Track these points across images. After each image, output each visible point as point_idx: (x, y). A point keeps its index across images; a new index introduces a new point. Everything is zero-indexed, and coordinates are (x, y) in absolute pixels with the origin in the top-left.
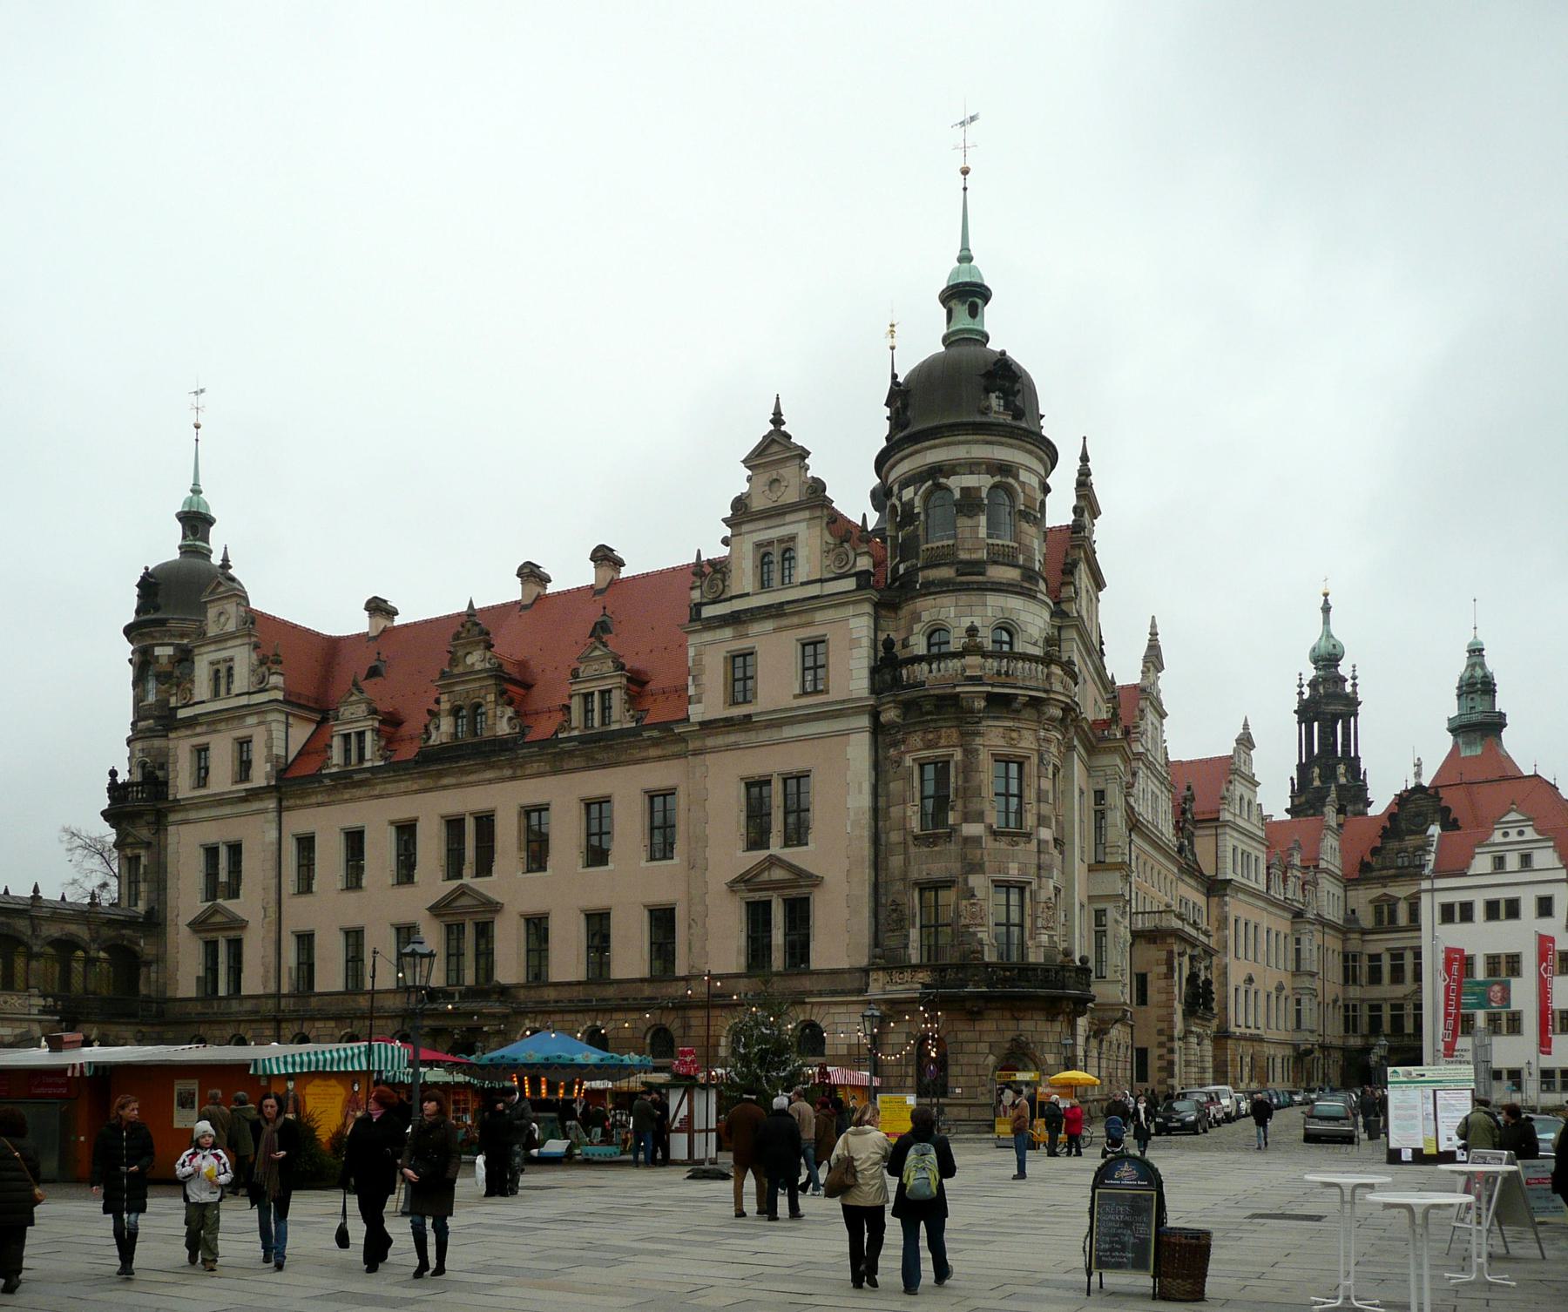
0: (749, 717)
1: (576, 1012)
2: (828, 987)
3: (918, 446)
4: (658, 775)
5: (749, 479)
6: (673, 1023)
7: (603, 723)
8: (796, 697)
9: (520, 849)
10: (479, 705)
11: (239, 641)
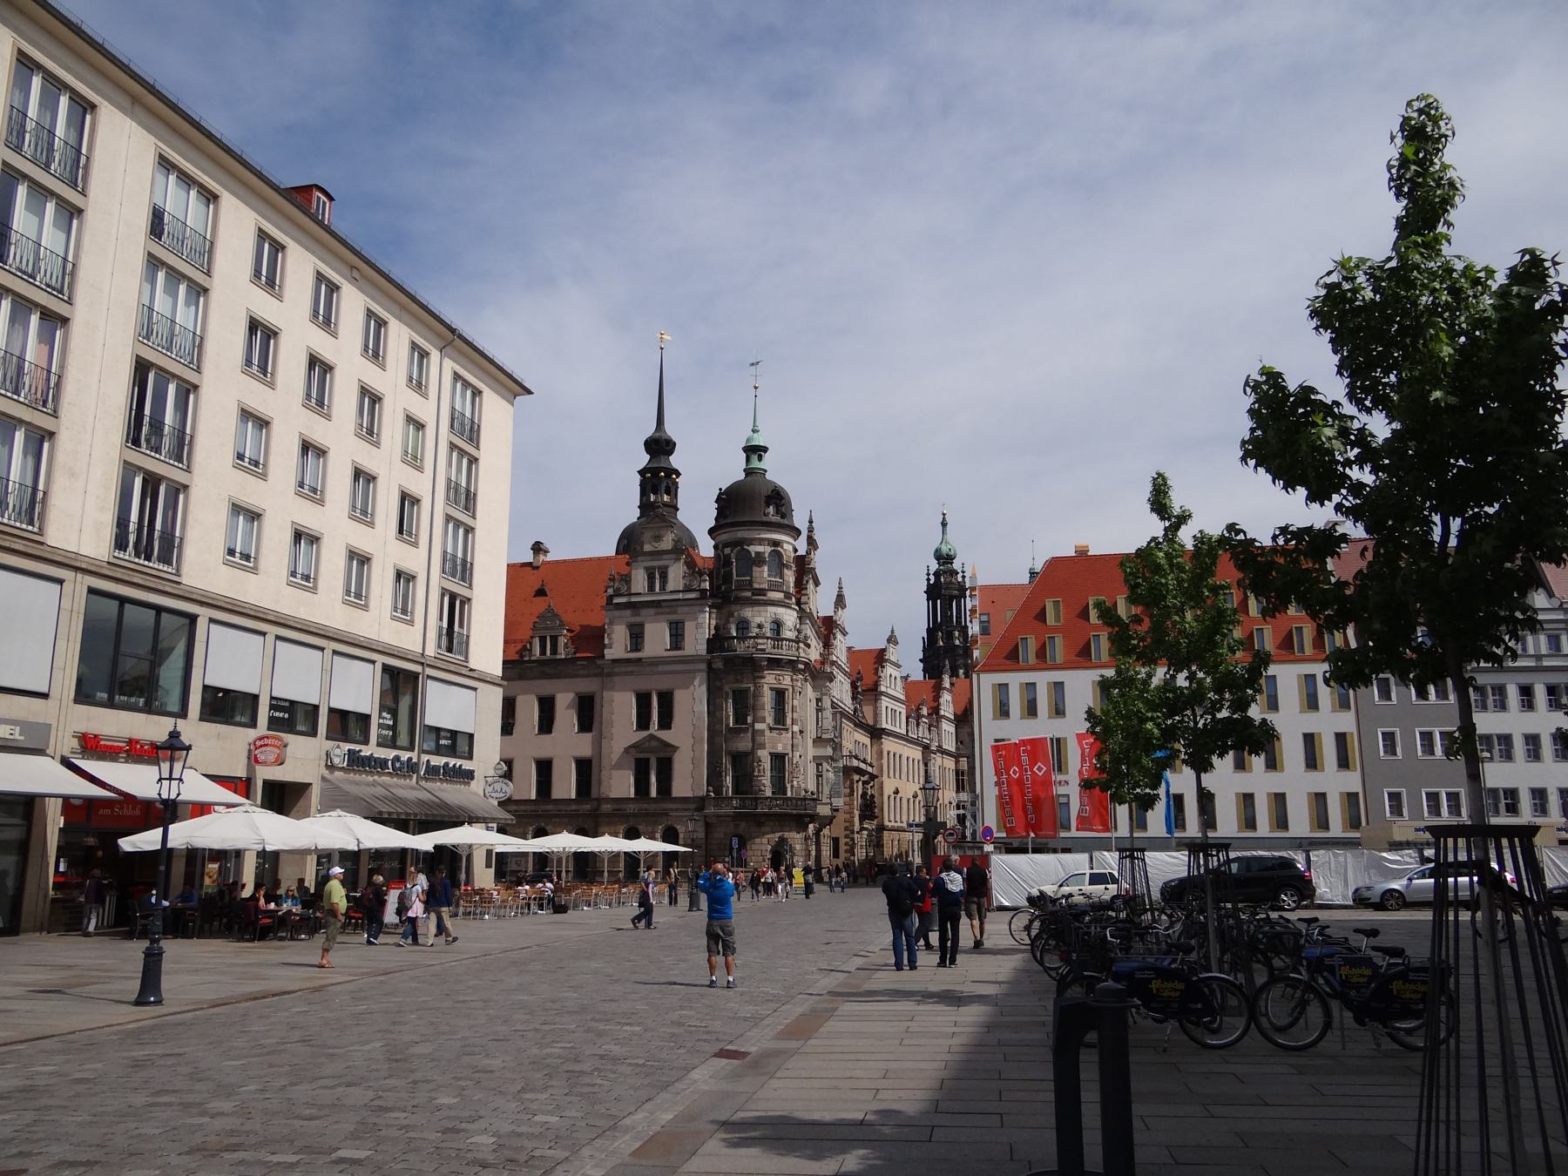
0: (640, 660)
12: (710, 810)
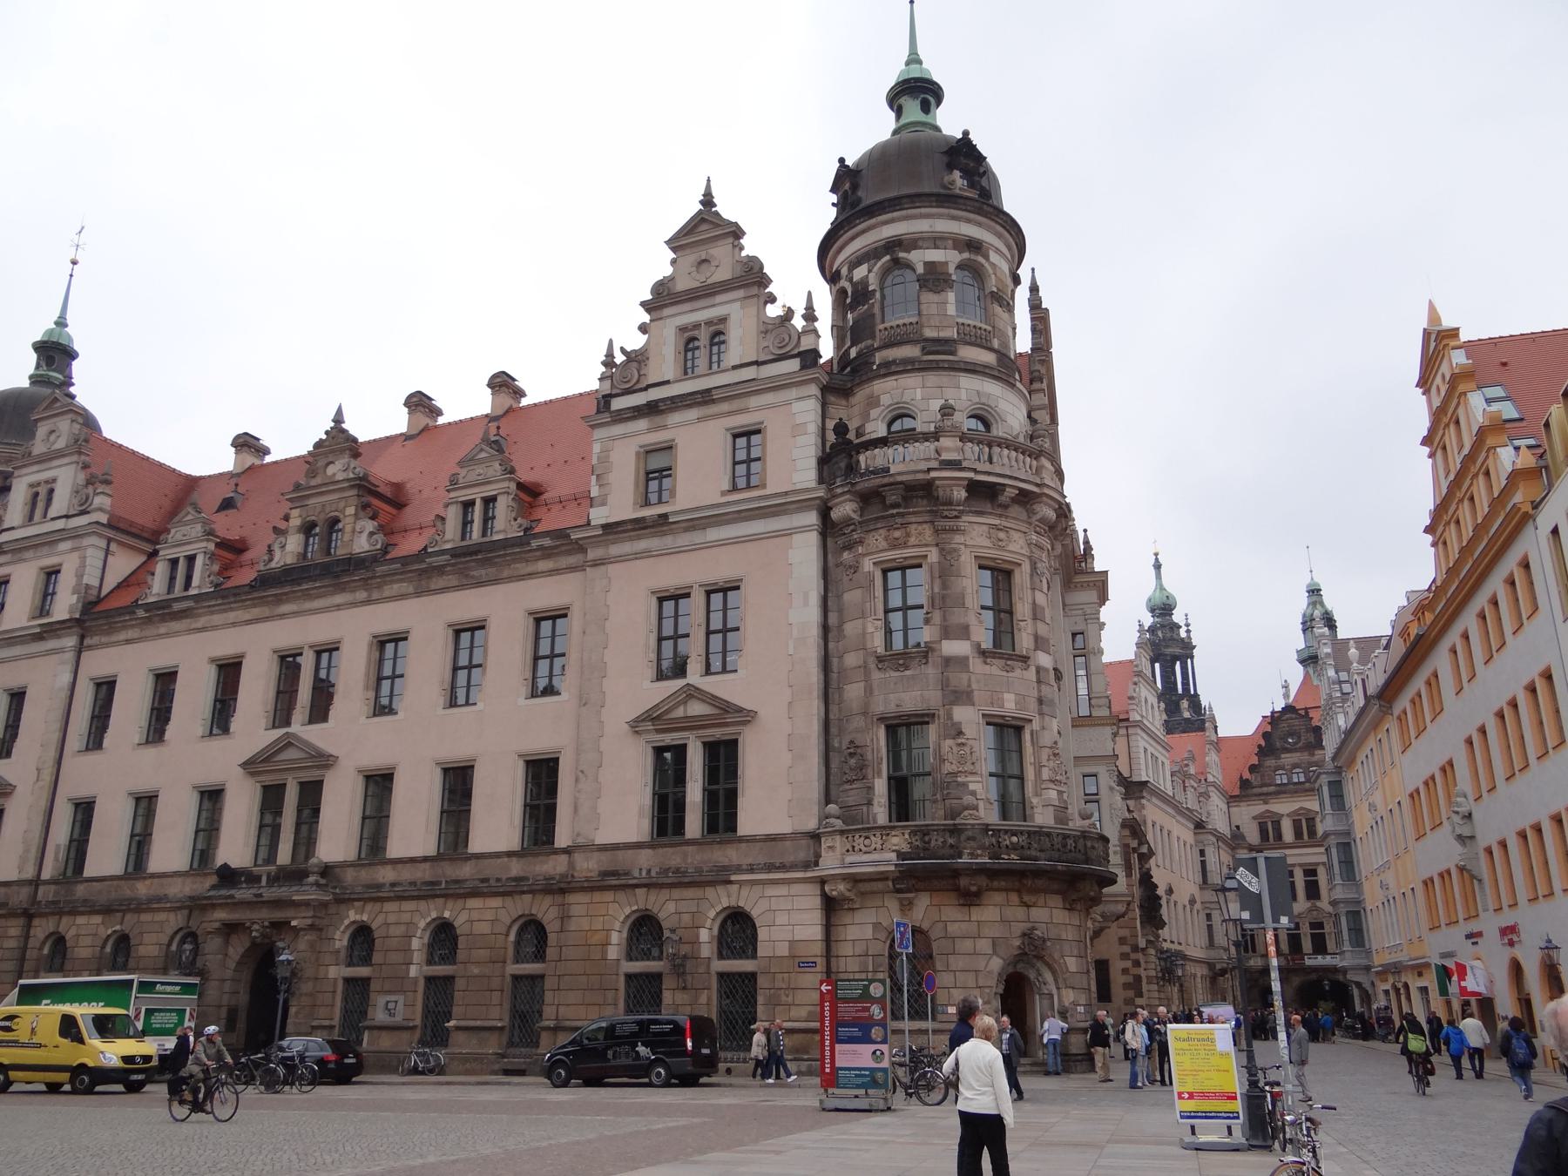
0: (664, 516)
1: (418, 898)
2: (762, 860)
3: (873, 221)
4: (544, 592)
5: (673, 262)
6: (546, 910)
7: (484, 534)
8: (724, 493)
9: (367, 688)
10: (336, 521)
11: (66, 460)
12: (833, 860)
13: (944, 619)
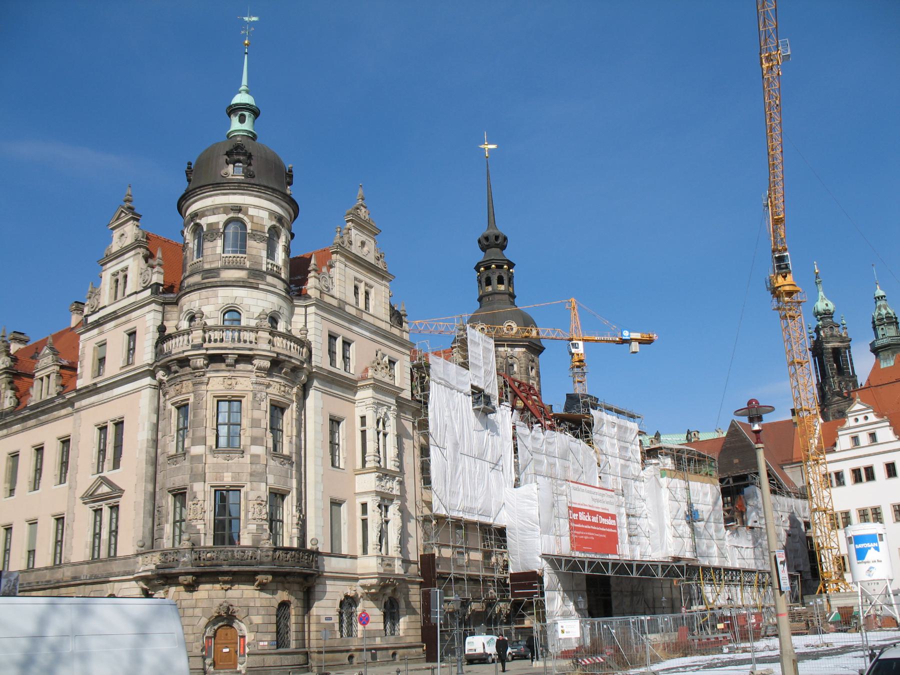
13: (193, 435)
